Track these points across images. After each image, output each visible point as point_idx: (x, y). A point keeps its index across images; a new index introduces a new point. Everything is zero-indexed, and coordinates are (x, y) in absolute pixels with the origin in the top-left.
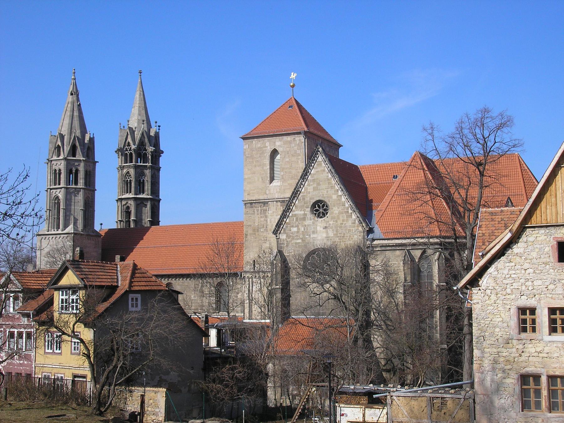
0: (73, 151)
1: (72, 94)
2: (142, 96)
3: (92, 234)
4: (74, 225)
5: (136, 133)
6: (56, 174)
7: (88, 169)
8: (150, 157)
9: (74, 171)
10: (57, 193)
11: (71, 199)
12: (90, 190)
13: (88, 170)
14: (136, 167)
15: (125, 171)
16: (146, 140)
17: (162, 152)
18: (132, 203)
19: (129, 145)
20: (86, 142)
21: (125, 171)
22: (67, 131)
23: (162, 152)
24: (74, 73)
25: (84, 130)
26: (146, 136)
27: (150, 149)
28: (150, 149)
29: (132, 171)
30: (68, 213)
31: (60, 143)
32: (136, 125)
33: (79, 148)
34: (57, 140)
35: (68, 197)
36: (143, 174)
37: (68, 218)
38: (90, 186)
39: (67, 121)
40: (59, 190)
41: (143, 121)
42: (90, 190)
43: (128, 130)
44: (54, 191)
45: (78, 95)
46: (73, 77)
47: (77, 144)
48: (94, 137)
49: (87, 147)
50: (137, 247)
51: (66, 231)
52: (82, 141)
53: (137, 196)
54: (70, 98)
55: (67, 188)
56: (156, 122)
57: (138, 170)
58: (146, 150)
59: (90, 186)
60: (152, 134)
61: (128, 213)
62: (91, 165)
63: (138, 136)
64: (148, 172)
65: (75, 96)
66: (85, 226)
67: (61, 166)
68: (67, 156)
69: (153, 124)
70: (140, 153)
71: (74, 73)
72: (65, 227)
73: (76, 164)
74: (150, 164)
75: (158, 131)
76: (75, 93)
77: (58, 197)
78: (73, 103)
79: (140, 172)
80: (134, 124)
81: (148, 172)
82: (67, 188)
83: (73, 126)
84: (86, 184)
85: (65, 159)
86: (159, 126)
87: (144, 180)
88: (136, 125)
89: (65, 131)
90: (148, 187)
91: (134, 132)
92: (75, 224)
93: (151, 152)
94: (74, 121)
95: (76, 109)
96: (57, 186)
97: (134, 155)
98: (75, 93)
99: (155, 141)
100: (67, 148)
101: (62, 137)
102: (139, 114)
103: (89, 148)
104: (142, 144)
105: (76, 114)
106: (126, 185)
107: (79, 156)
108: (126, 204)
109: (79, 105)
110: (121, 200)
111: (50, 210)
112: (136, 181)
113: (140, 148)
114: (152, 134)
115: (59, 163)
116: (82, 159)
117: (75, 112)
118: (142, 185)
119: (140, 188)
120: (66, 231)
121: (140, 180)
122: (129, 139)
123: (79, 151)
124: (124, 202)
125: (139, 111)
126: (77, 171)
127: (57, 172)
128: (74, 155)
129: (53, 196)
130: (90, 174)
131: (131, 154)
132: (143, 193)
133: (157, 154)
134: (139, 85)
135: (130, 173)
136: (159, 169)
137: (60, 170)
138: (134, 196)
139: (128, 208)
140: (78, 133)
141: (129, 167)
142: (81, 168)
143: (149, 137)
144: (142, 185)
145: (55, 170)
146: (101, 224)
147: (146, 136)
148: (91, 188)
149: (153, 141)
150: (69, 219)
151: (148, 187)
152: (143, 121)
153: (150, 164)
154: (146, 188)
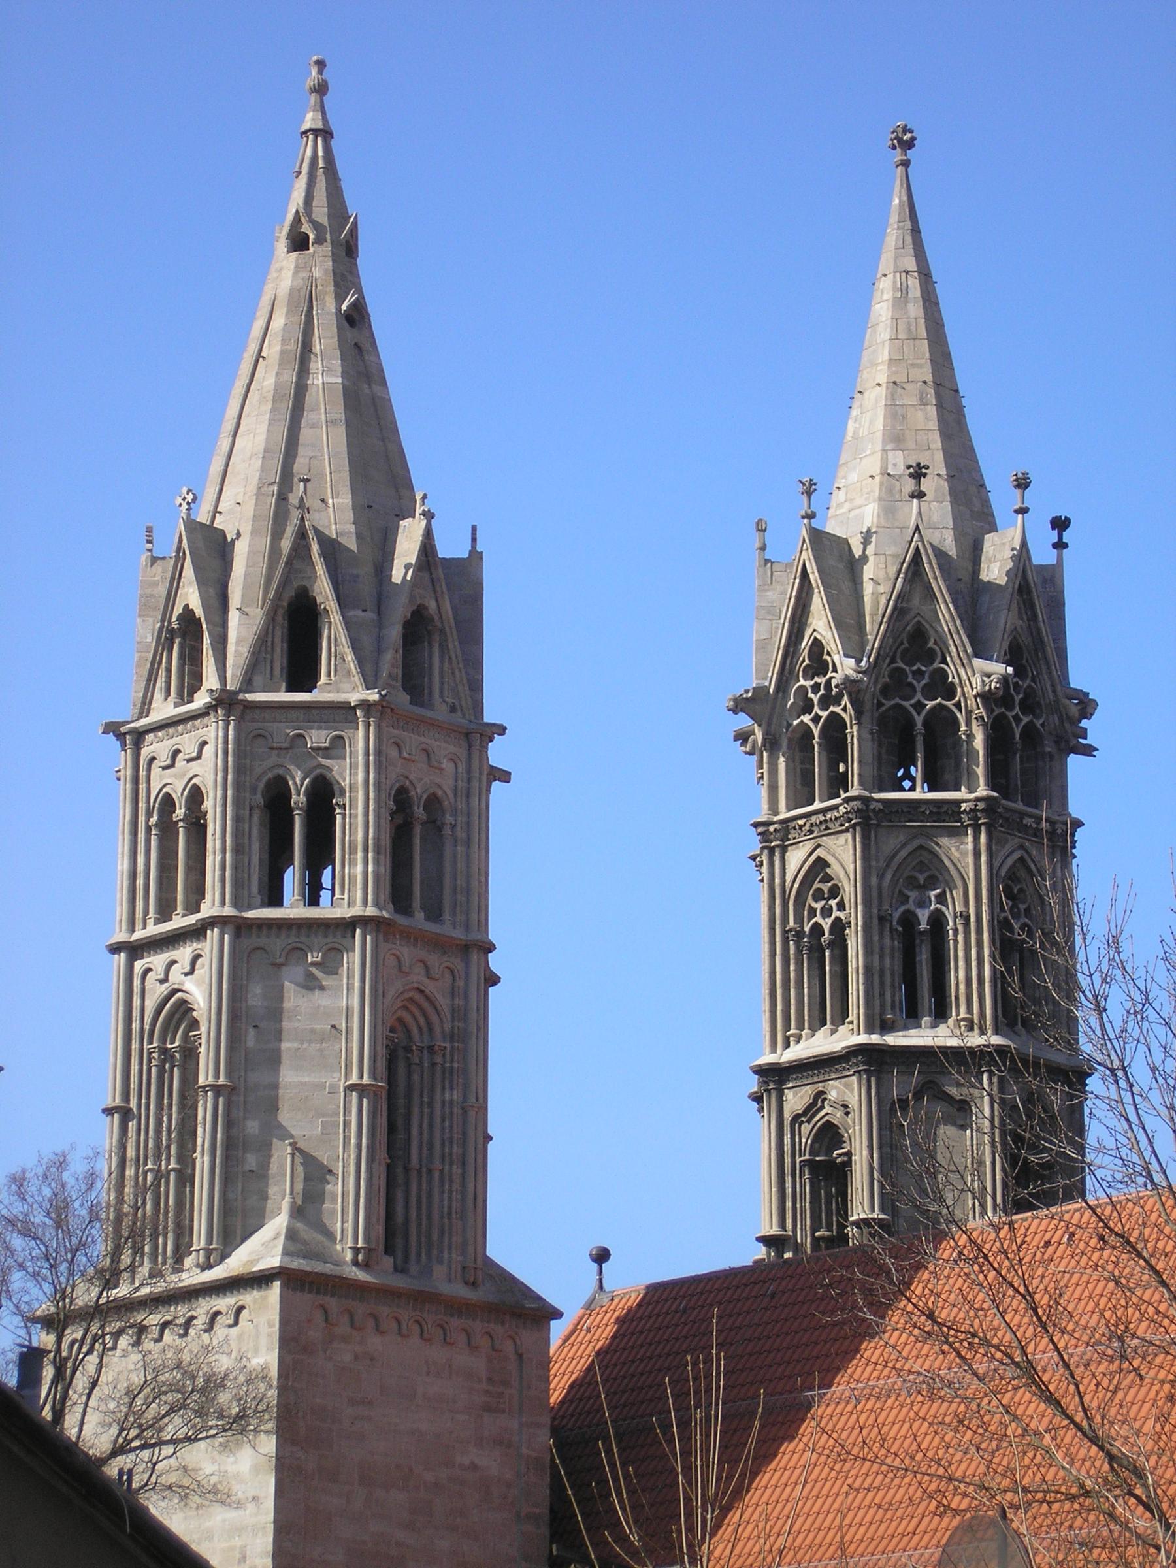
0: (295, 640)
1: (299, 243)
2: (915, 310)
3: (461, 1291)
4: (297, 1212)
5: (868, 571)
6: (174, 828)
7: (422, 783)
8: (979, 743)
9: (298, 798)
10: (176, 975)
11: (276, 1013)
12: (440, 945)
13: (419, 792)
14: (870, 821)
15: (796, 858)
16: (946, 614)
17: (1086, 706)
18: (847, 1093)
19: (819, 663)
20: (397, 574)
21: (796, 858)
22: (249, 508)
23: (1086, 706)
24: (321, 89)
25: (383, 480)
26: (939, 585)
27: (977, 675)
28: (977, 675)
29: (844, 854)
30: (253, 1127)
31: (191, 596)
32: (870, 515)
33: (336, 617)
34: (176, 578)
35: (256, 996)
36: (930, 873)
37: (251, 1161)
38: (434, 914)
39: (257, 435)
40: (183, 954)
41: (918, 473)
42: (440, 945)
43: (807, 556)
44: (157, 961)
45: (347, 251)
46: (310, 120)
47: (323, 590)
48: (476, 556)
49: (399, 612)
50: (840, 1388)
51: (238, 1262)
52: (365, 571)
53: (892, 1040)
54: (284, 271)
55: (239, 928)
56: (1022, 483)
57: (891, 842)
58: (950, 692)
59: (434, 914)
60: (995, 568)
61: (827, 1173)
62: (445, 749)
63: (878, 584)
64: (964, 854)
65: (320, 260)
66: (393, 1233)
67: (199, 760)
68: (248, 684)
69: (1002, 497)
70: (902, 714)
71: (321, 89)
72: (234, 1227)
73: (317, 737)
74: (982, 791)
75: (1042, 555)
76: (330, 235)
77: (183, 1010)
78: (304, 305)
79: (903, 855)
80: (854, 508)
81: (964, 854)
82: (239, 928)
83: (300, 466)
84: (398, 885)
85: (225, 702)
86: (1061, 524)
87: (938, 921)
88: (870, 515)
89: (239, 511)
90: (970, 965)
91: (854, 566)
92: (308, 1208)
93: (986, 697)
94: (305, 434)
95: (326, 340)
96: (179, 922)
97: (853, 731)
98: (330, 235)
99: (1031, 617)
100: (242, 628)
101: (212, 550)
102: (895, 438)
103: (418, 628)
104: (910, 648)
105: (327, 376)
106: (809, 956)
107: (342, 681)
108: (811, 1110)
109: (355, 319)
110: (774, 1077)
111: (125, 1114)
112: (876, 921)
113: (898, 676)
114: (995, 568)
115: (187, 742)
116: (354, 698)
117: (316, 365)
118: (924, 956)
119: (913, 972)
120: (238, 1262)
121: (909, 920)
122: (820, 624)
123: (335, 635)
124: (795, 1099)
125: (895, 413)
126: (323, 796)
127: (180, 812)
128: (302, 673)
129: (151, 1004)
130: (434, 825)
131: (835, 726)
132: (941, 1014)
133: (1040, 726)
134: (894, 235)
135: (835, 869)
136: (1061, 838)
137: (196, 796)
138: (863, 1039)
139: (830, 1135)
140: (336, 514)
141: (824, 827)
142: (355, 774)
143: (972, 595)
144: (924, 956)
145: (168, 803)
146: (601, 1256)
147: (939, 585)
148: (448, 929)
149: (1004, 621)
150: (261, 1175)
151: (970, 965)
152: (918, 473)
153: (982, 791)
154: (957, 977)
